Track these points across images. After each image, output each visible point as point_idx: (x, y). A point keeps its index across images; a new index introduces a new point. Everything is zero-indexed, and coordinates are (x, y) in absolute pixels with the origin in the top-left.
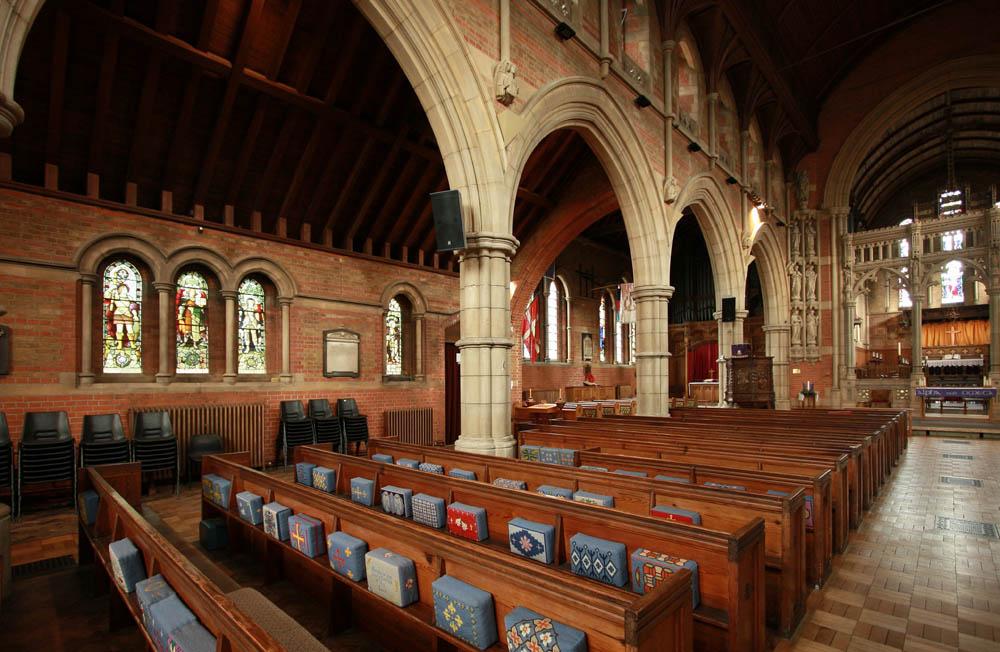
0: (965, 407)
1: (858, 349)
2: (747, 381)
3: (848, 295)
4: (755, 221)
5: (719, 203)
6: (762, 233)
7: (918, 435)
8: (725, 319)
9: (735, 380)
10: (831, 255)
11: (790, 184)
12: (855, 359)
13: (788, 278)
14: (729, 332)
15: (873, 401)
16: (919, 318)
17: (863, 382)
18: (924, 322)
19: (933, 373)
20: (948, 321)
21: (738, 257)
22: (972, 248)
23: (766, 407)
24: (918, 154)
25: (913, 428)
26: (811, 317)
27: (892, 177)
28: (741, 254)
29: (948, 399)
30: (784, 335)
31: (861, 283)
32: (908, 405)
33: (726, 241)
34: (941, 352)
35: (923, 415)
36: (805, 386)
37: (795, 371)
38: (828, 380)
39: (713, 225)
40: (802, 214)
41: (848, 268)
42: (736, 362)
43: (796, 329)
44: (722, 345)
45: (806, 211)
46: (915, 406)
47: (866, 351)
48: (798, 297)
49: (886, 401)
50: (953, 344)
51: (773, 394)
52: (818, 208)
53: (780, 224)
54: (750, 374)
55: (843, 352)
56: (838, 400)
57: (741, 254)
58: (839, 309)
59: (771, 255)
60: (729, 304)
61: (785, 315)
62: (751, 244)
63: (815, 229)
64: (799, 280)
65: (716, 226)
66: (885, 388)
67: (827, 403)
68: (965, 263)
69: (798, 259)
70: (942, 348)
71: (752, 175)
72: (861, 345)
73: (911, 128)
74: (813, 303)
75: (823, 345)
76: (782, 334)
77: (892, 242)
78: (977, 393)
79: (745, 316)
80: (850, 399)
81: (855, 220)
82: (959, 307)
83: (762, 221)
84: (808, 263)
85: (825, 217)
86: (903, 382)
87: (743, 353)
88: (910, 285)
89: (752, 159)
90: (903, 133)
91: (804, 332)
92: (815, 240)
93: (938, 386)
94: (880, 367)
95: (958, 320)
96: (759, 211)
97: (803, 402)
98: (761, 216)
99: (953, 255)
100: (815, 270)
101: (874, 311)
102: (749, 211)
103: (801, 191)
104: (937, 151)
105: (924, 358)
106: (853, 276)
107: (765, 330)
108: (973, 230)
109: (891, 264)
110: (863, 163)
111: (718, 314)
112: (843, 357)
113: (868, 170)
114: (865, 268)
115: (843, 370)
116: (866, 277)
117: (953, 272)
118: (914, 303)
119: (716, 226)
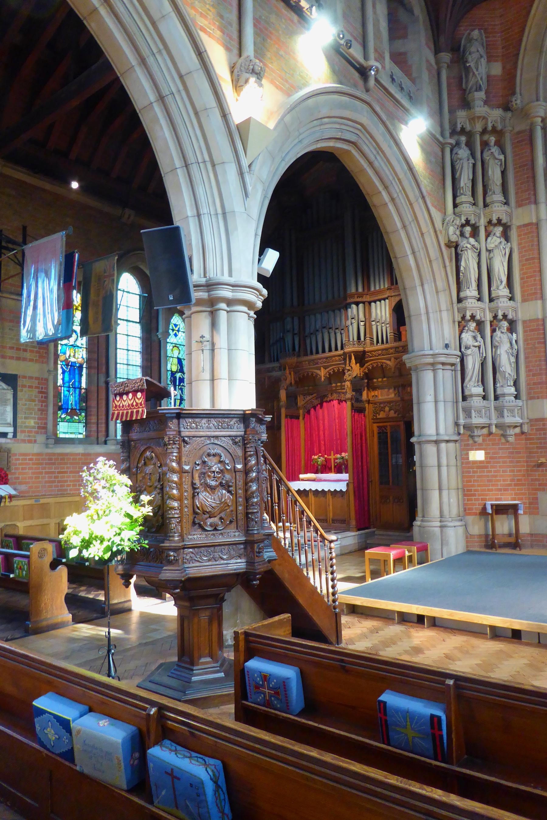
37: (478, 455)
43: (472, 364)
48: (471, 292)
63: (503, 152)
75: (531, 397)
91: (490, 370)
92: (503, 173)
100: (506, 236)
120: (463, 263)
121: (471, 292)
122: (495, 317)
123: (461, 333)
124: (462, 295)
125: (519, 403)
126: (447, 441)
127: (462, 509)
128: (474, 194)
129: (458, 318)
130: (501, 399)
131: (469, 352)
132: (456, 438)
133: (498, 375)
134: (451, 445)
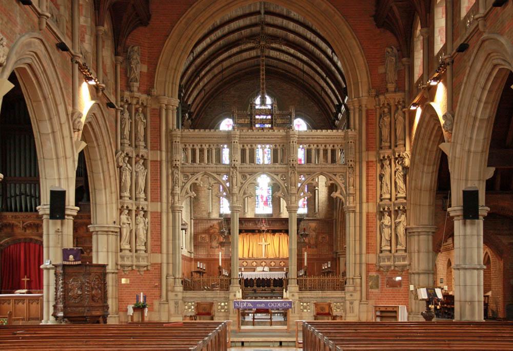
0: (271, 319)
1: (184, 258)
2: (79, 292)
3: (176, 198)
4: (86, 102)
5: (49, 72)
6: (92, 114)
7: (236, 346)
8: (53, 216)
9: (66, 290)
10: (161, 150)
11: (120, 58)
12: (181, 271)
13: (117, 170)
14: (57, 231)
15: (199, 314)
16: (236, 226)
17: (189, 294)
18: (241, 232)
19: (247, 284)
20: (260, 232)
21: (68, 140)
22: (277, 165)
23: (98, 322)
24: (238, 53)
25: (232, 339)
26: (140, 218)
27: (216, 71)
28: (71, 138)
29: (259, 311)
30: (112, 238)
31: (188, 186)
32: (227, 317)
33: (55, 120)
34: (254, 264)
35: (239, 327)
36: (138, 298)
39: (41, 99)
40: (132, 97)
41: (176, 167)
42: (70, 270)
43: (125, 232)
44: (48, 247)
45: (137, 94)
46: (233, 319)
47: (190, 260)
48: (127, 194)
49: (209, 314)
50: (263, 257)
51: (107, 307)
52: (148, 93)
53: (110, 105)
54: (83, 284)
55: (171, 261)
56: (166, 313)
57: (71, 138)
58: (168, 213)
59: (100, 140)
60: (58, 197)
61: (115, 213)
62: (82, 128)
64: (128, 173)
65: (45, 98)
66: (209, 300)
67: (155, 318)
68: (273, 179)
69: (128, 149)
70: (255, 260)
71: (82, 40)
72: (185, 252)
73: (234, 25)
74: (142, 203)
76: (110, 236)
77: (215, 146)
78: (279, 305)
79: (75, 213)
80: (177, 313)
81: (182, 111)
82: (270, 219)
83: (92, 99)
84: (137, 156)
85: (156, 106)
86: (222, 294)
87: (75, 259)
88: (230, 195)
89: (84, 20)
90: (226, 29)
93: (252, 298)
94: (205, 278)
95: (268, 231)
96: (90, 87)
97: (132, 317)
98: (91, 94)
99: (263, 169)
101: (199, 216)
102: (80, 85)
103: (131, 69)
104: (253, 53)
105: (240, 269)
106: (180, 177)
107: (91, 230)
108: (278, 147)
109: (214, 169)
110: (192, 52)
111: (44, 208)
112: (171, 266)
113: (195, 59)
114: (191, 170)
115: (171, 280)
116: (193, 180)
117: (264, 183)
118: (233, 213)
119: (45, 98)
120: (124, 177)
121: (127, 194)
122: (138, 208)
123: (120, 214)
124: (122, 194)
126: (113, 273)
127: (117, 309)
128: (130, 139)
129: (120, 207)
130: (139, 252)
131: (125, 226)
132: (116, 271)
133: (137, 240)
134: (114, 275)
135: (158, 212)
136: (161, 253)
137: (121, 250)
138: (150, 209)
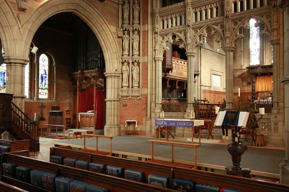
10: (148, 24)
38: (144, 112)
43: (125, 76)
48: (126, 53)
91: (130, 78)
92: (139, 13)
115: (153, 105)
125: (139, 89)
126: (114, 101)
127: (119, 122)
134: (116, 102)
135: (145, 62)
136: (147, 88)
137: (122, 87)
138: (141, 61)
